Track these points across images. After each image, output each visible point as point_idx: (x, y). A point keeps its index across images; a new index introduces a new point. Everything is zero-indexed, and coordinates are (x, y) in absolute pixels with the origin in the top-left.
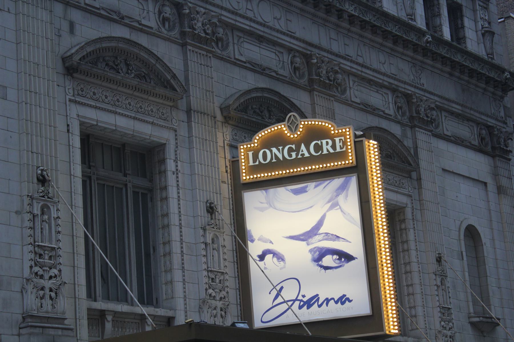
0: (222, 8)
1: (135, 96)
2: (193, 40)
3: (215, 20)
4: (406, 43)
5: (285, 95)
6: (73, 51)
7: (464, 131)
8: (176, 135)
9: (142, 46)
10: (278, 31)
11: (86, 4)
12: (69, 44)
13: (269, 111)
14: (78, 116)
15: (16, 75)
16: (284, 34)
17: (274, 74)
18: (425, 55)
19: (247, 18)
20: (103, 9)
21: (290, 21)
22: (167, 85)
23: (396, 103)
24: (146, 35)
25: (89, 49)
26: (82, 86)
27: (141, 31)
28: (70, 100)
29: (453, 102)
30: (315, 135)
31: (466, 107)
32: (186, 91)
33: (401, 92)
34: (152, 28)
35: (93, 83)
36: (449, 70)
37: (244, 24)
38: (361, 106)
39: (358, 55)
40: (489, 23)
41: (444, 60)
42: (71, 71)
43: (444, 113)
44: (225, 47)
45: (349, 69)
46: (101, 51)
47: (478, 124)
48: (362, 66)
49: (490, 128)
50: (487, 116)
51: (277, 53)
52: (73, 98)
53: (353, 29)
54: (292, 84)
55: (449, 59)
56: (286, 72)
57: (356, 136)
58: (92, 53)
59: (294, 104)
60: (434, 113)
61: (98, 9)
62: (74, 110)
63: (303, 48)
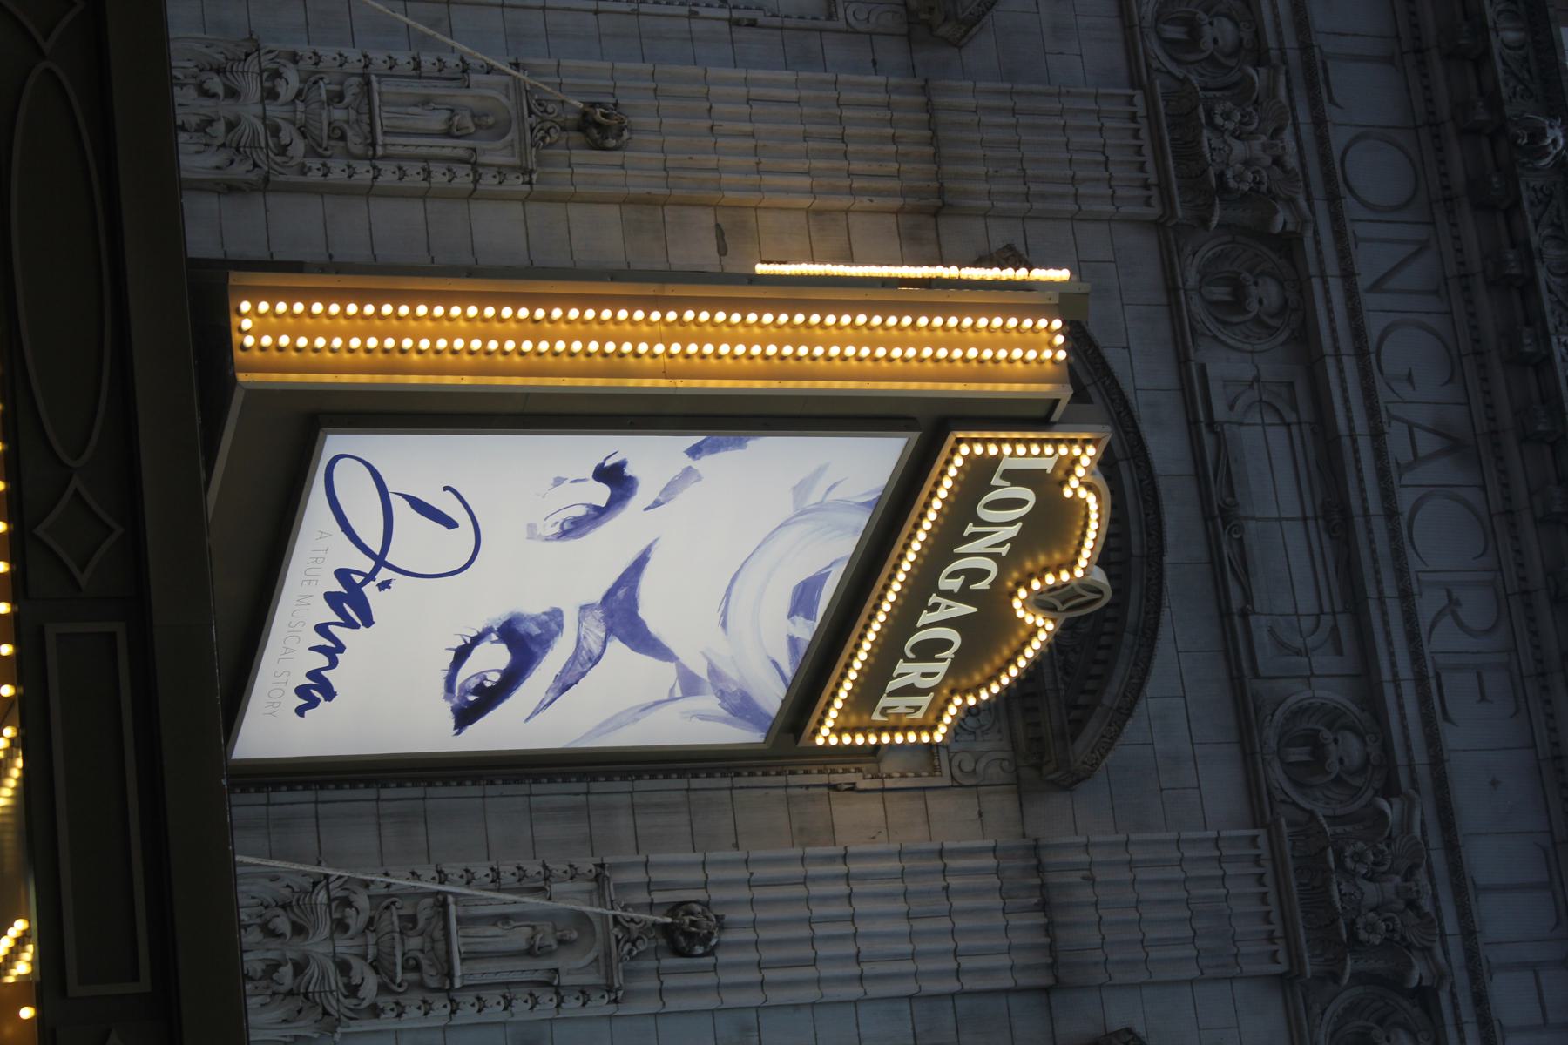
5: (1170, 574)
16: (1413, 636)
19: (1372, 411)
51: (1326, 621)
59: (1154, 639)
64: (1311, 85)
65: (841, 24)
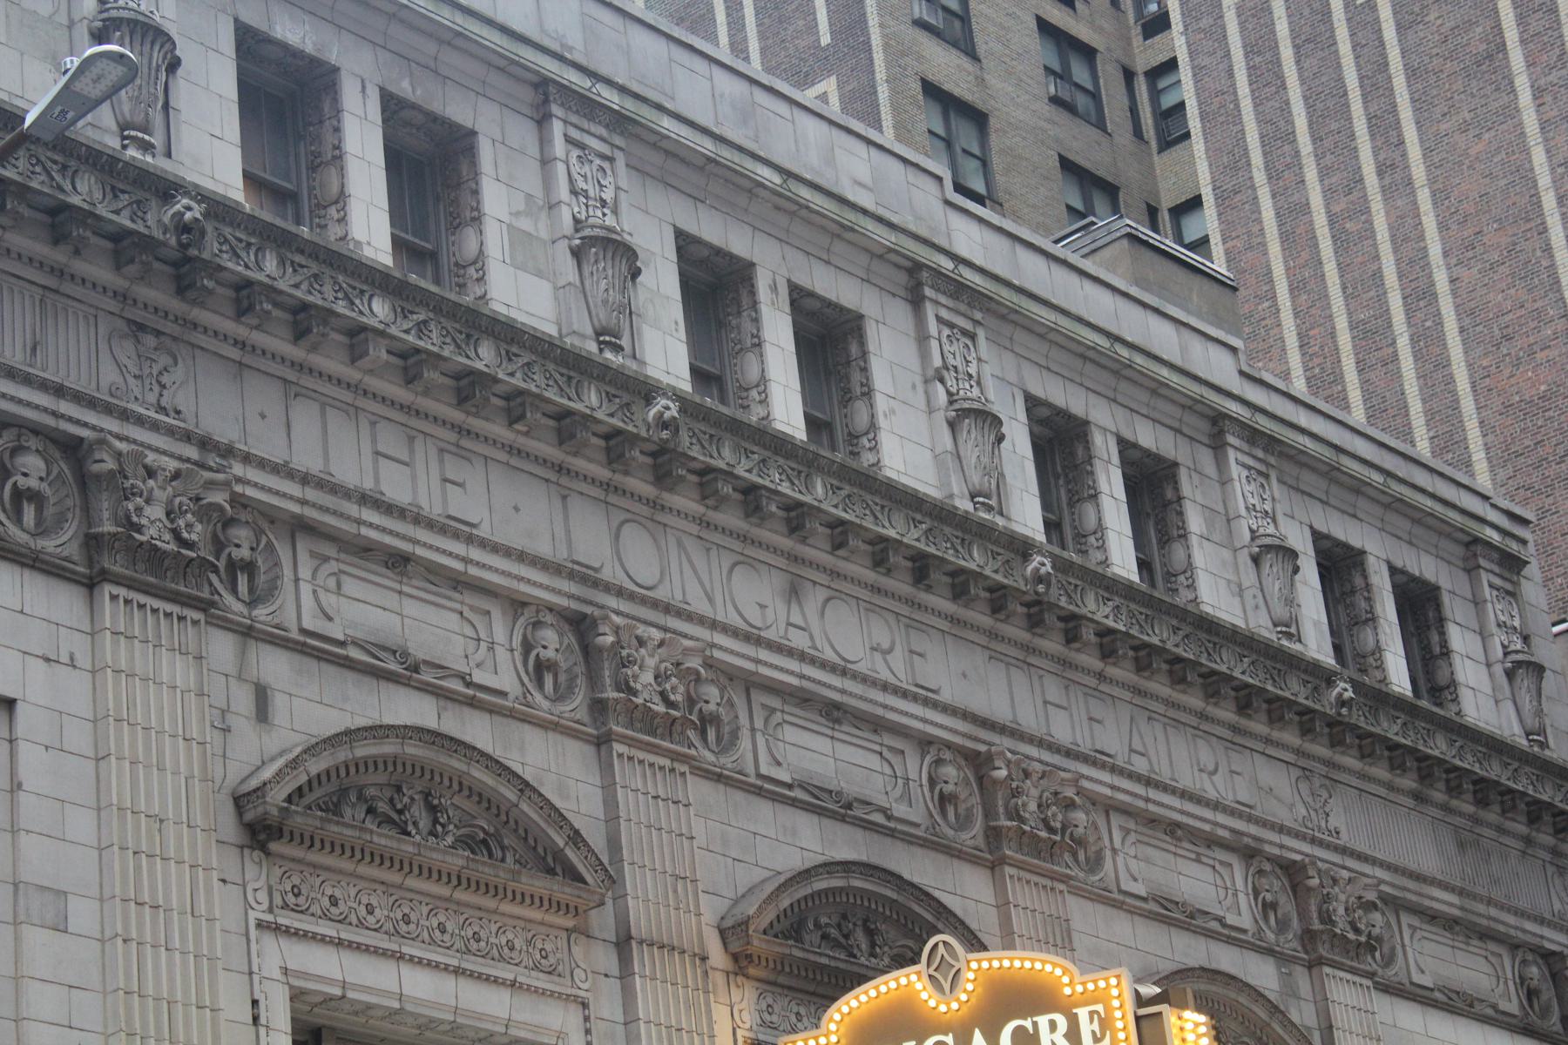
0: (714, 625)
1: (458, 903)
2: (630, 724)
3: (694, 663)
4: (1277, 710)
5: (916, 880)
6: (267, 774)
7: (1472, 970)
8: (587, 1019)
9: (475, 748)
10: (885, 687)
11: (303, 631)
12: (256, 753)
13: (871, 933)
14: (285, 971)
15: (96, 853)
16: (905, 694)
17: (878, 818)
18: (1335, 743)
19: (790, 652)
20: (355, 643)
21: (920, 655)
22: (555, 865)
23: (1256, 893)
24: (487, 716)
25: (316, 766)
26: (296, 880)
27: (472, 703)
28: (260, 925)
29: (1433, 882)
30: (1014, 999)
31: (1474, 897)
32: (613, 881)
33: (1270, 859)
34: (503, 694)
35: (328, 869)
36: (1414, 785)
37: (782, 670)
38: (1152, 906)
39: (1131, 750)
40: (1526, 639)
41: (1397, 756)
42: (262, 837)
43: (1406, 919)
44: (727, 743)
45: (1108, 792)
46: (352, 770)
47: (1515, 947)
48: (1148, 782)
49: (1548, 957)
50: (1542, 921)
51: (886, 753)
52: (270, 918)
53: (1113, 671)
54: (934, 844)
55: (1413, 751)
56: (915, 811)
57: (1141, 1001)
58: (324, 778)
59: (945, 907)
60: (1377, 917)
61: (342, 644)
62: (274, 955)
63: (964, 735)
64: (596, 584)
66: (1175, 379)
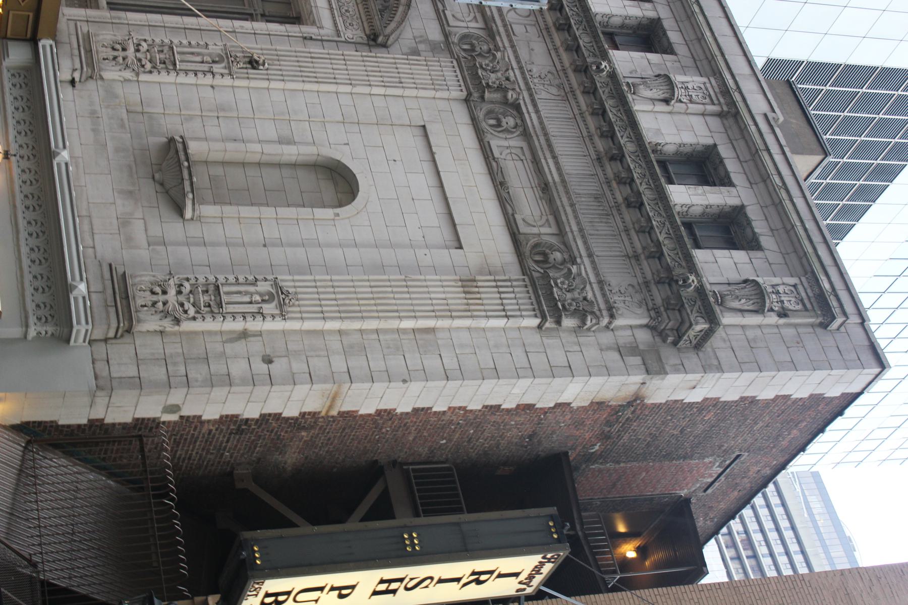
7: (529, 206)
36: (602, 150)
47: (561, 233)
65: (343, 39)
66: (710, 39)
